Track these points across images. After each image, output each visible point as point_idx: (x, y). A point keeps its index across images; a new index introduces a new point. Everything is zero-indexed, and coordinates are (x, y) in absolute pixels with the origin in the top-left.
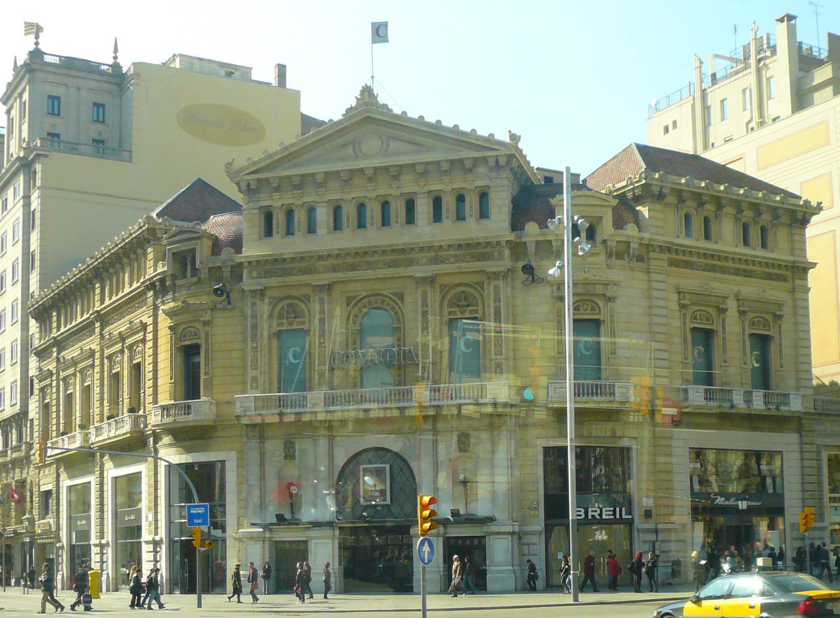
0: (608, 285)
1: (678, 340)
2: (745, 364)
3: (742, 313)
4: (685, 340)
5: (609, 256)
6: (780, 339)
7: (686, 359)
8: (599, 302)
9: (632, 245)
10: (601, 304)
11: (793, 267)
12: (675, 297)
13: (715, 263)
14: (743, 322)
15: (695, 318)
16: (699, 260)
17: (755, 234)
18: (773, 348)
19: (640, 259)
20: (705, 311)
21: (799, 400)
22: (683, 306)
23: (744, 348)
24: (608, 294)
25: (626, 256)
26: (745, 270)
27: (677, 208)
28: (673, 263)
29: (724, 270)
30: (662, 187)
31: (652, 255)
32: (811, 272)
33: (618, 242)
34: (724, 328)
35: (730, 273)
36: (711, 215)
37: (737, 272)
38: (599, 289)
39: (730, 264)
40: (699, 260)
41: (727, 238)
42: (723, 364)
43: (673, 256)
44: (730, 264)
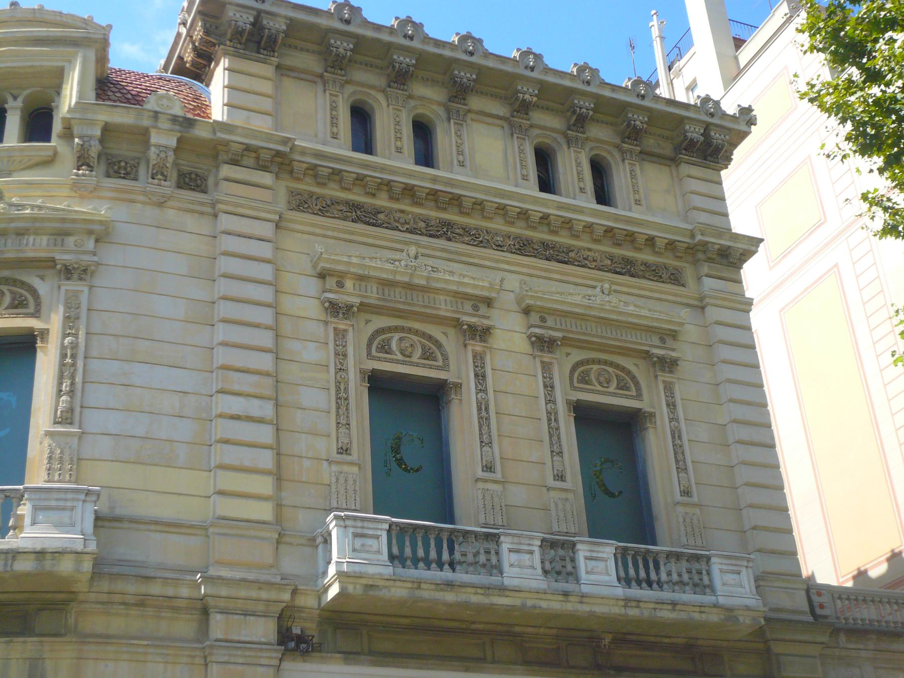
0: (67, 234)
1: (313, 399)
2: (560, 477)
3: (543, 343)
4: (342, 400)
5: (83, 161)
6: (674, 419)
7: (344, 450)
8: (36, 282)
9: (154, 139)
10: (43, 288)
11: (692, 250)
12: (312, 286)
13: (450, 220)
14: (546, 367)
15: (385, 348)
16: (396, 206)
17: (572, 167)
18: (656, 446)
19: (192, 181)
20: (416, 332)
21: (746, 578)
22: (334, 309)
23: (554, 432)
24: (63, 257)
25: (142, 171)
26: (545, 245)
27: (325, 83)
28: (301, 203)
29: (477, 238)
30: (259, 14)
31: (226, 170)
32: (753, 275)
33: (107, 129)
34: (480, 377)
35: (499, 247)
36: (434, 112)
37: (523, 247)
38: (37, 246)
39: (497, 225)
40: (396, 206)
41: (487, 160)
42: (480, 474)
43: (307, 186)
44: (497, 225)
